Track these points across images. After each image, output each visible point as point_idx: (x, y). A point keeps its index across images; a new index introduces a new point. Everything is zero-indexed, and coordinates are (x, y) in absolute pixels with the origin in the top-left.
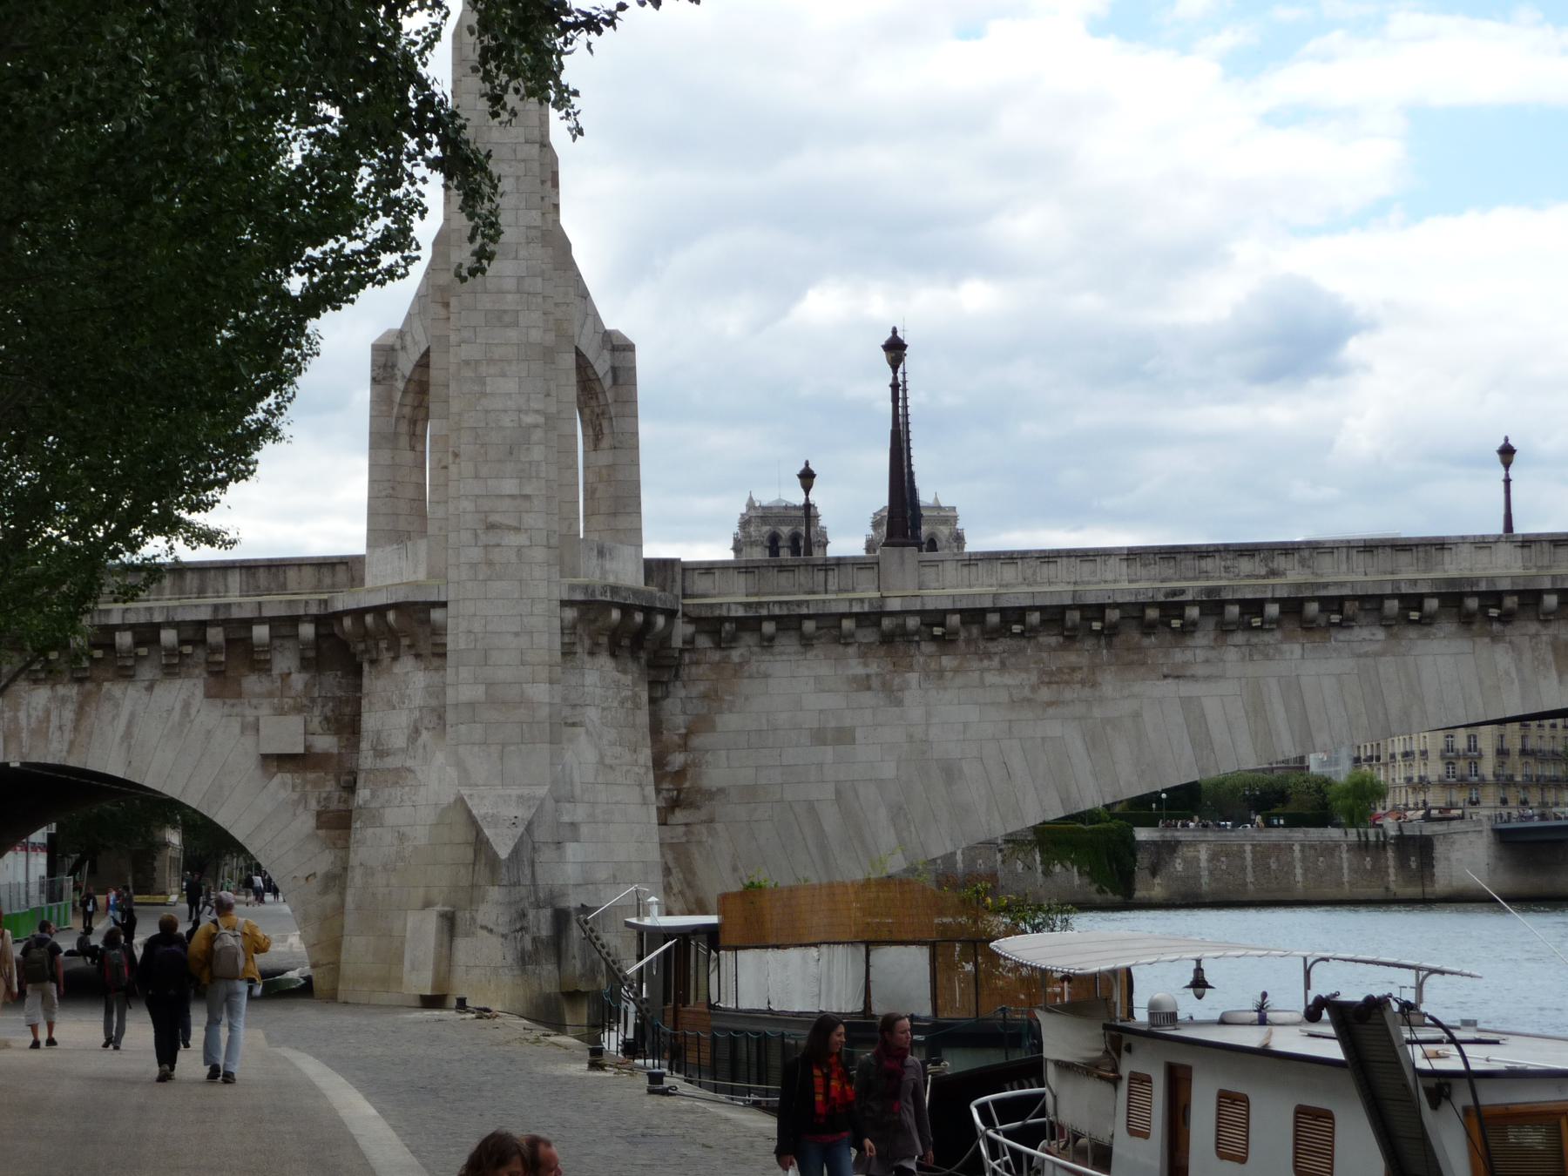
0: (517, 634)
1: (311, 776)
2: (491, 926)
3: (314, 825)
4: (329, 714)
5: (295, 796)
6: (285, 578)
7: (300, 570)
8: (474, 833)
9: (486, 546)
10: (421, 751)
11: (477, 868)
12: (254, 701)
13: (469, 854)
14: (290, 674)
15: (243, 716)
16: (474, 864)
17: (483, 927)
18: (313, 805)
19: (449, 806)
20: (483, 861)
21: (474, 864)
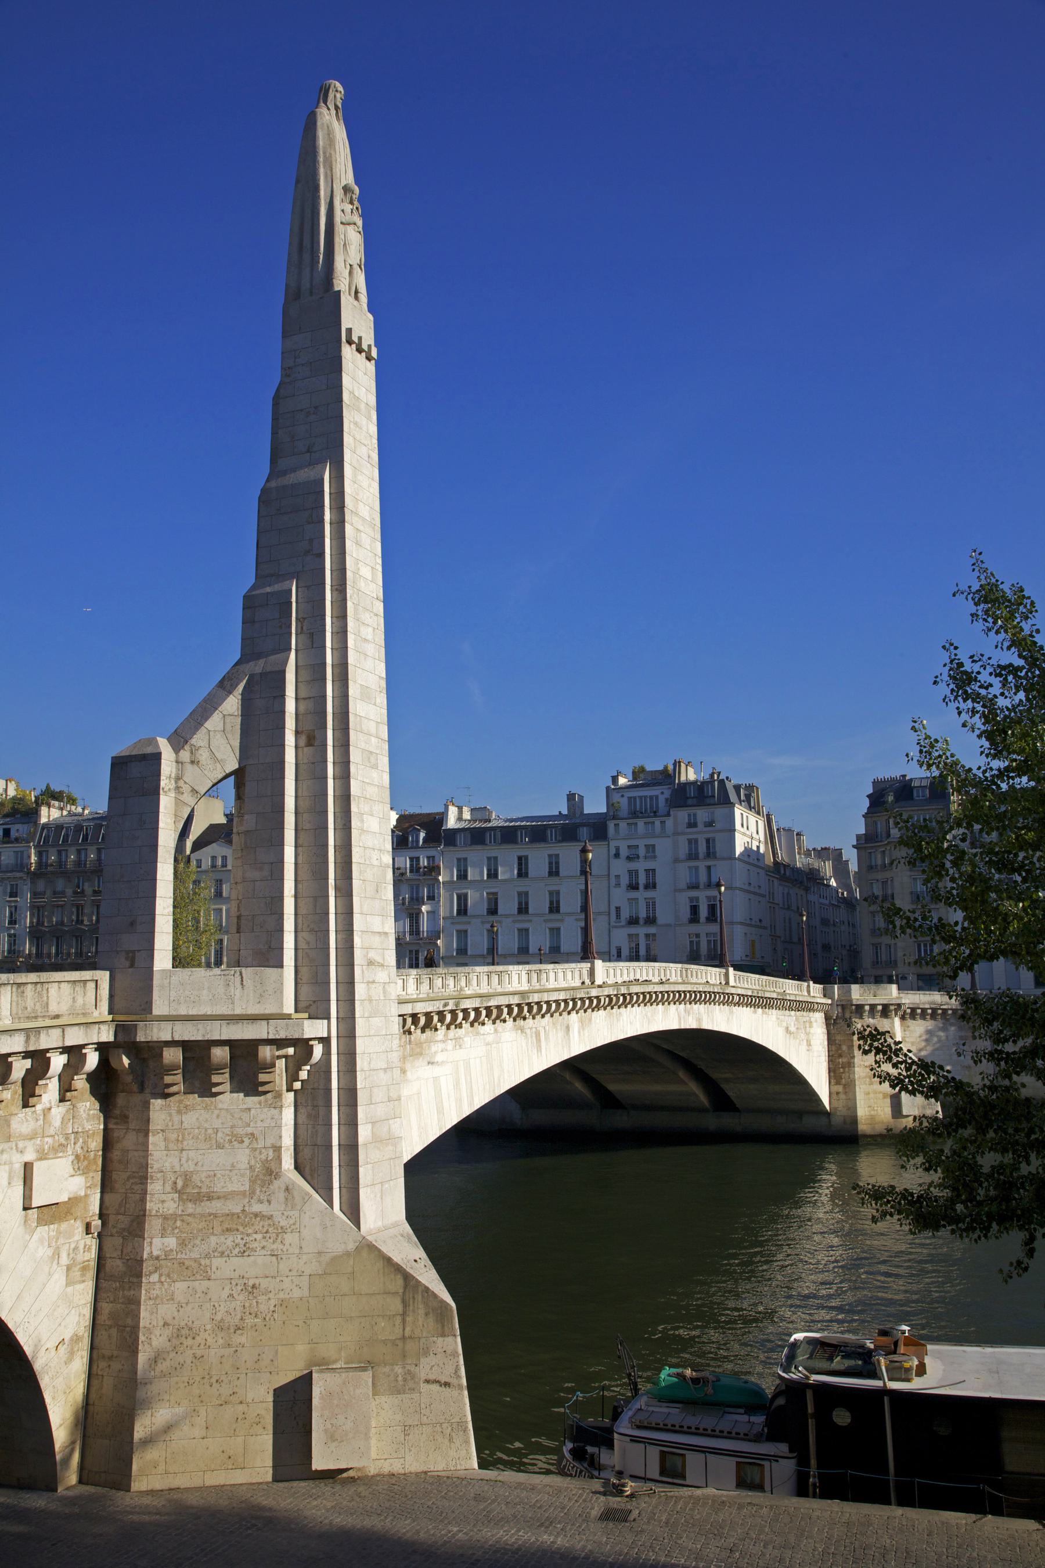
0: (385, 1070)
1: (64, 1226)
2: (443, 1379)
3: (64, 1283)
4: (79, 1151)
5: (50, 1252)
6: (48, 997)
7: (85, 986)
8: (400, 1281)
9: (368, 982)
10: (281, 1196)
11: (409, 1319)
12: (21, 1145)
13: (395, 1305)
14: (50, 1109)
15: (11, 1163)
16: (404, 1315)
17: (427, 1381)
18: (64, 1260)
19: (348, 1254)
20: (421, 1311)
21: (404, 1315)
